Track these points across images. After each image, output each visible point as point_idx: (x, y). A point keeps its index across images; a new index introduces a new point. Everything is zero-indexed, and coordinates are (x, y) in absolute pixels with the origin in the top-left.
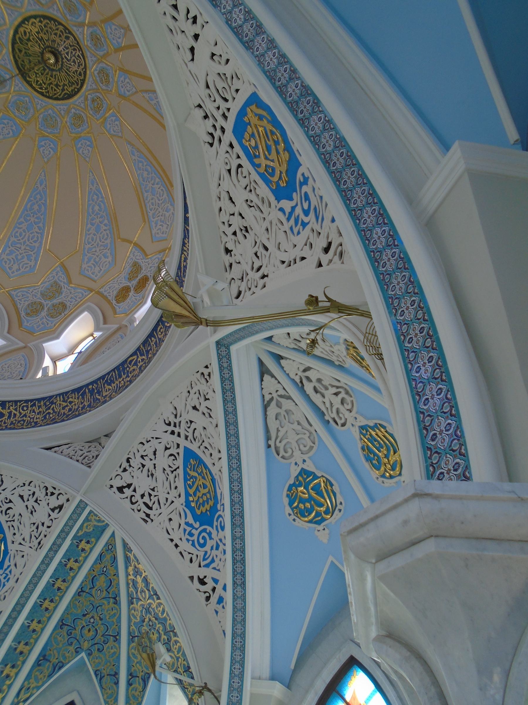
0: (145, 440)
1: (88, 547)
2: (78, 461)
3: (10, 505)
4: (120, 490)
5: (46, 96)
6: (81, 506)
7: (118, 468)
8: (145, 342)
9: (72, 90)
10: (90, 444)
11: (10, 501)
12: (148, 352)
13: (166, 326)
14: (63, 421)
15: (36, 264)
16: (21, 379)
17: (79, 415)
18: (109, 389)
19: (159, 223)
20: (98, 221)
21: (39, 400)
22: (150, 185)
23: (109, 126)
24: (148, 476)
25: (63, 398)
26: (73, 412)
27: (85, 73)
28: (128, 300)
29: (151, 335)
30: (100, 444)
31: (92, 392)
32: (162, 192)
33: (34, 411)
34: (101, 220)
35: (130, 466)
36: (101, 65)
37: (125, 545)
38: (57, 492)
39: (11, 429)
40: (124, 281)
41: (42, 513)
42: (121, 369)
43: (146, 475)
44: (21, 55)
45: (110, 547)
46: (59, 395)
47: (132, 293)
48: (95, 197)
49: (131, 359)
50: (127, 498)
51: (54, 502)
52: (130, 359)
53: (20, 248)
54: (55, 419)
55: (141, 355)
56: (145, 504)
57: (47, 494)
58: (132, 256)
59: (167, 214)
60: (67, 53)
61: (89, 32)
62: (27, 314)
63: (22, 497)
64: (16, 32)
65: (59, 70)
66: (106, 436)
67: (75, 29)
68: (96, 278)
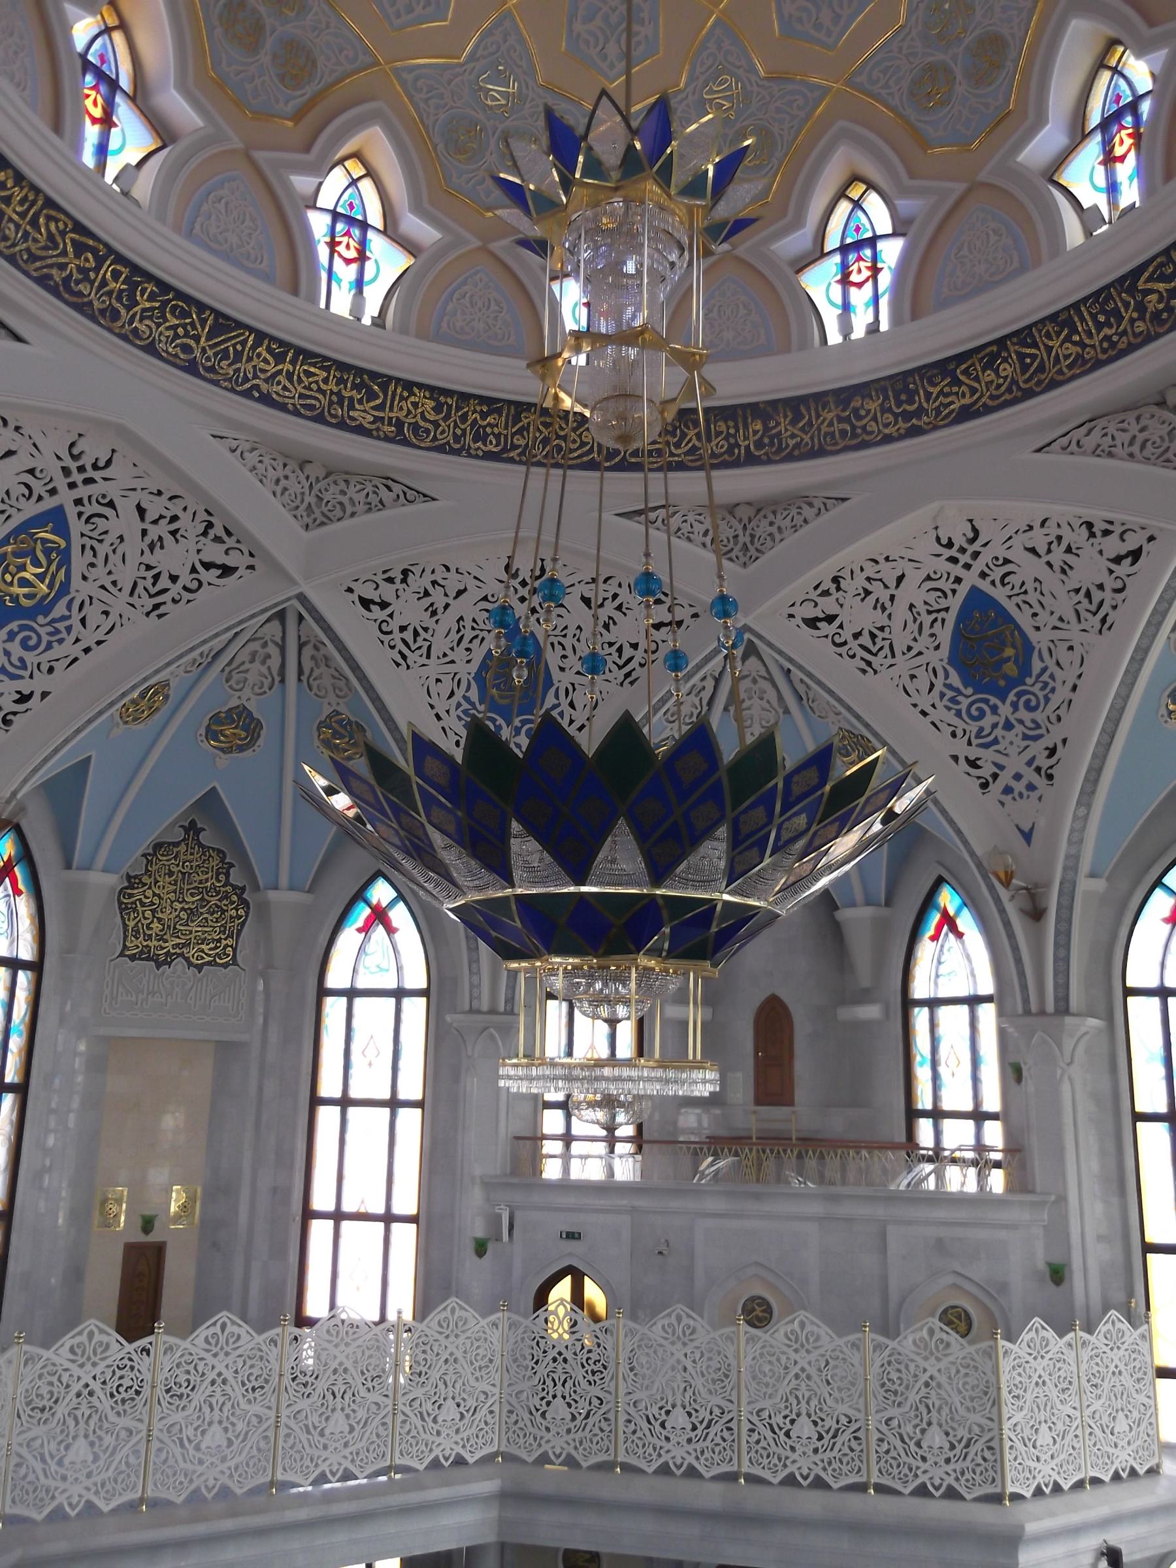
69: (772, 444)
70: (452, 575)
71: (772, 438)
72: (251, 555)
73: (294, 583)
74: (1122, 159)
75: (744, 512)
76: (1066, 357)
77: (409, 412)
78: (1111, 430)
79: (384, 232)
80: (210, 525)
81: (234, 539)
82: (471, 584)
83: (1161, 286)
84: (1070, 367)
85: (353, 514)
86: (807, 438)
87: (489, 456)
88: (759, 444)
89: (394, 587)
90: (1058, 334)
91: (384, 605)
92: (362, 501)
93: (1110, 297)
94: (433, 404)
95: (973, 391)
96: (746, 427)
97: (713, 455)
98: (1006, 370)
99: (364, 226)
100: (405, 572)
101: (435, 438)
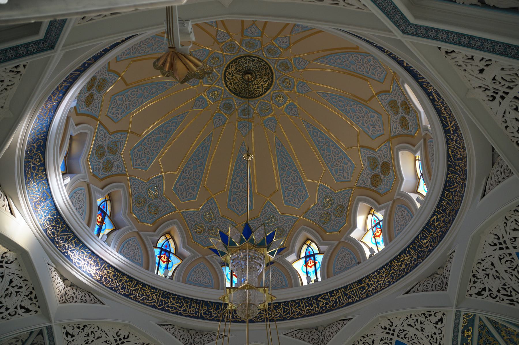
0: (480, 259)
1: (470, 333)
2: (433, 290)
3: (405, 332)
4: (479, 294)
5: (255, 97)
6: (458, 315)
7: (469, 283)
8: (438, 207)
9: (268, 85)
10: (431, 277)
11: (404, 331)
12: (444, 211)
13: (452, 192)
14: (407, 273)
15: (306, 192)
16: (359, 263)
17: (416, 266)
18: (427, 242)
19: (371, 127)
20: (325, 146)
21: (381, 269)
22: (348, 108)
23: (300, 90)
24: (495, 279)
25: (396, 260)
26: (410, 265)
27: (272, 71)
28: (383, 183)
29: (441, 200)
30: (437, 274)
31: (414, 249)
32: (360, 109)
33: (382, 276)
34: (327, 144)
35: (478, 279)
36: (279, 62)
37: (491, 321)
38: (433, 313)
39: (376, 293)
40: (370, 172)
41: (430, 329)
42: (428, 227)
43: (493, 278)
44: (232, 86)
45: (482, 327)
46: (393, 260)
47: (382, 177)
48: (315, 134)
49: (432, 219)
50: (487, 296)
51: (434, 319)
52: (432, 219)
53: (292, 188)
54: (399, 275)
55: (439, 214)
56: (503, 295)
57: (426, 317)
58: (364, 155)
59: (374, 119)
60: (256, 68)
61: (265, 50)
62: (323, 223)
63: (410, 325)
64: (225, 76)
65: (255, 79)
66: (440, 268)
67: (256, 53)
68: (349, 180)
69: (208, 314)
70: (99, 331)
71: (209, 312)
72: (39, 307)
73: (50, 321)
74: (311, 267)
75: (193, 332)
76: (296, 312)
77: (106, 274)
78: (304, 333)
79: (109, 217)
80: (31, 293)
81: (36, 300)
82: (104, 335)
83: (324, 301)
84: (297, 315)
85: (76, 302)
86: (219, 315)
87: (125, 295)
88: (205, 314)
89: (78, 330)
90: (295, 305)
91: (72, 336)
92: (80, 298)
93: (310, 300)
94: (113, 273)
95: (269, 314)
96: (202, 307)
97: (191, 313)
98: (279, 311)
99: (105, 214)
100: (85, 326)
101: (110, 285)
